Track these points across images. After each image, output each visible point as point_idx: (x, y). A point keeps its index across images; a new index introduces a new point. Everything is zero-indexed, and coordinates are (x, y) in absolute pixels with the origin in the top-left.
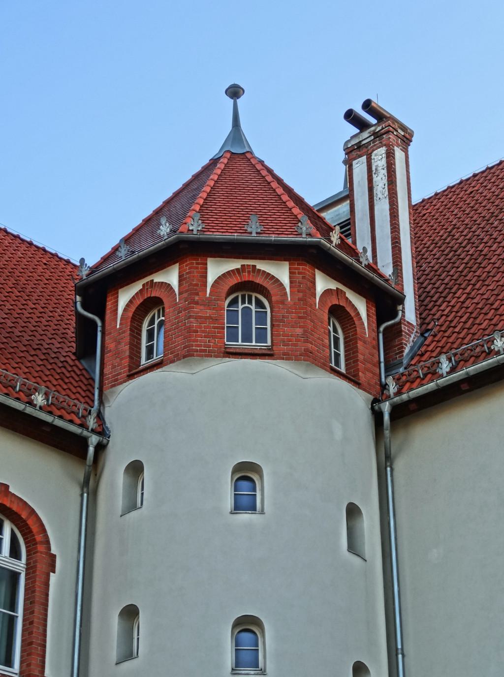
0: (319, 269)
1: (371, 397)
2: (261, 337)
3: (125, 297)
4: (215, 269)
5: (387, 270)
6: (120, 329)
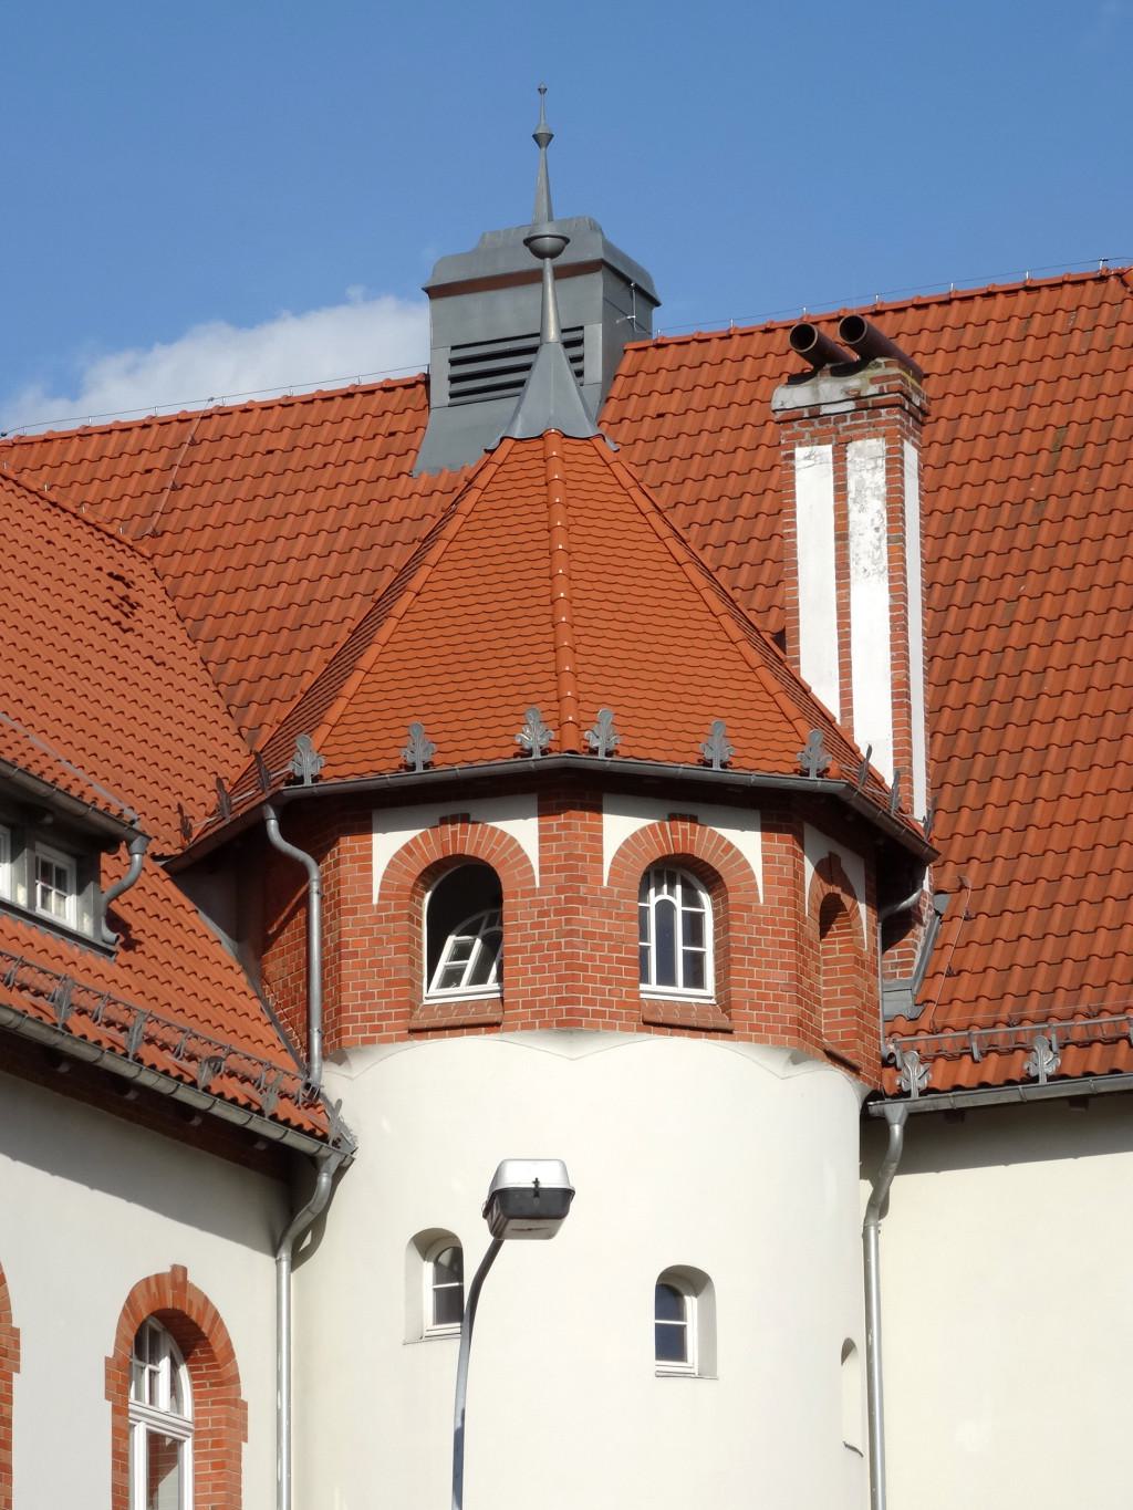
0: (812, 823)
1: (869, 1089)
2: (695, 978)
3: (386, 845)
4: (618, 829)
5: (884, 765)
6: (380, 908)
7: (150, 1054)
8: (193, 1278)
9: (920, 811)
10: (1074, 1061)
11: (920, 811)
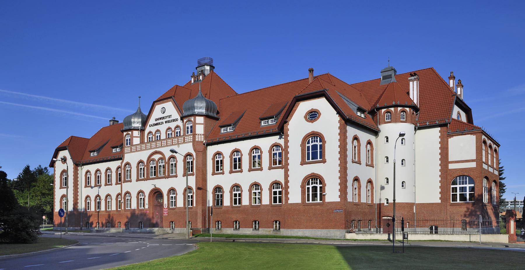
7: (361, 122)
8: (371, 140)
9: (418, 107)
10: (430, 123)
11: (418, 107)
